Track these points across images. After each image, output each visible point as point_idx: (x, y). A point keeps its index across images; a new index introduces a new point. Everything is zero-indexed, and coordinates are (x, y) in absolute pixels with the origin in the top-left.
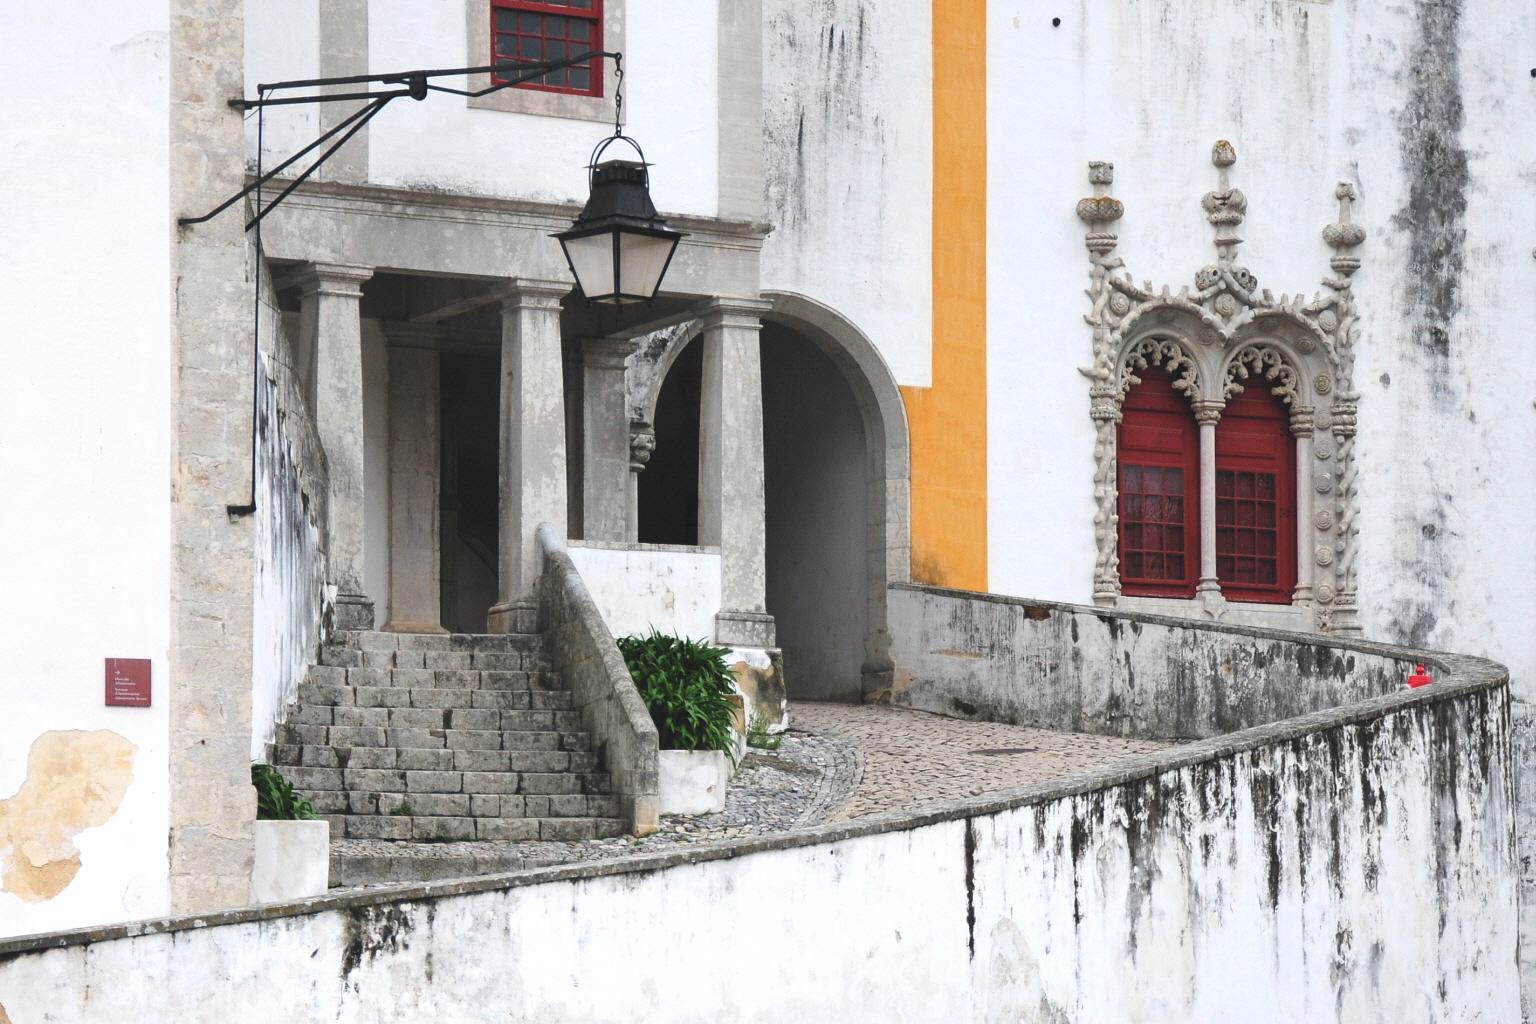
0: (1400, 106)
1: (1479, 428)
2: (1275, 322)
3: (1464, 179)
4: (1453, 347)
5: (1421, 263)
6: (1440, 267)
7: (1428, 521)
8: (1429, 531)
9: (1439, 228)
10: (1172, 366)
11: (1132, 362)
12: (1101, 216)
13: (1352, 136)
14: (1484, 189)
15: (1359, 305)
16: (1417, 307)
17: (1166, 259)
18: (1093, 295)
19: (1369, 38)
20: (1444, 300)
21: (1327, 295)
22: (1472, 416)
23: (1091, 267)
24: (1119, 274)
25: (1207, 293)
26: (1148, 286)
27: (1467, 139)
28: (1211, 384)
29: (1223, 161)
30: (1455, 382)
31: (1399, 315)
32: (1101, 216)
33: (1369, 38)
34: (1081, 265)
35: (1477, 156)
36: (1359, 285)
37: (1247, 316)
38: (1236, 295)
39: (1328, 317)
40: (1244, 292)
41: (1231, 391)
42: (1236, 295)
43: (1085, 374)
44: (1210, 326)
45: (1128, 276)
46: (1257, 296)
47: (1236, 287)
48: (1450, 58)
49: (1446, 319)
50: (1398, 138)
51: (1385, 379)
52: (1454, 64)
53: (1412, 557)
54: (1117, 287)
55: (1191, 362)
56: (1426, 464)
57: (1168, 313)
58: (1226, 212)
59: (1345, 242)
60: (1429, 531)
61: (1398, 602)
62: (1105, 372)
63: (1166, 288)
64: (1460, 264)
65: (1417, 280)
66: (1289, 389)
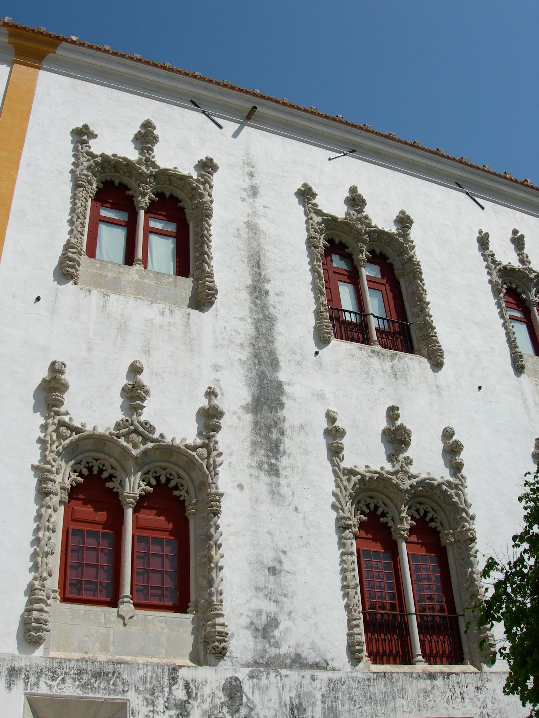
0: (244, 358)
1: (301, 516)
2: (169, 451)
3: (282, 393)
4: (282, 473)
5: (260, 430)
6: (272, 433)
7: (272, 564)
8: (273, 571)
9: (269, 415)
10: (105, 475)
13: (216, 368)
14: (293, 399)
15: (221, 447)
16: (259, 451)
19: (225, 328)
20: (275, 449)
22: (296, 509)
26: (83, 425)
27: (282, 376)
30: (285, 490)
31: (248, 455)
33: (225, 328)
35: (289, 384)
36: (219, 437)
37: (150, 445)
39: (204, 451)
41: (144, 490)
43: (34, 468)
45: (71, 419)
46: (156, 436)
47: (141, 429)
48: (272, 342)
49: (277, 459)
50: (243, 372)
51: (241, 487)
52: (273, 345)
53: (261, 585)
54: (61, 424)
55: (116, 473)
56: (269, 533)
57: (98, 441)
60: (273, 571)
61: (254, 611)
63: (94, 429)
64: (283, 433)
65: (258, 438)
66: (183, 493)
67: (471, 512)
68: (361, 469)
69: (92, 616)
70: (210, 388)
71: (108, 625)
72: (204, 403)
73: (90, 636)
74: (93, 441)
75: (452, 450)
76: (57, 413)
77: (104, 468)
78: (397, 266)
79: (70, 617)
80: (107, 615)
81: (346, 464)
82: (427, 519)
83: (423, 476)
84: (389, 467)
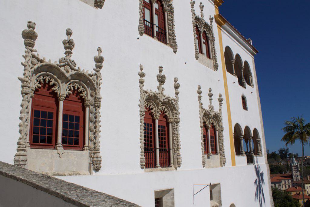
10: (52, 83)
11: (39, 80)
12: (30, 37)
17: (50, 51)
18: (25, 57)
21: (94, 72)
23: (26, 50)
24: (35, 53)
25: (63, 64)
28: (63, 90)
29: (69, 33)
32: (30, 37)
34: (24, 48)
36: (102, 71)
37: (73, 72)
38: (70, 66)
39: (95, 77)
40: (73, 66)
42: (70, 66)
44: (62, 74)
45: (38, 54)
46: (76, 68)
47: (71, 64)
54: (33, 56)
57: (50, 68)
58: (69, 45)
59: (99, 61)
62: (27, 79)
63: (50, 61)
67: (179, 111)
68: (149, 91)
69: (45, 154)
70: (99, 47)
71: (52, 158)
72: (96, 54)
73: (44, 164)
74: (48, 67)
75: (177, 87)
76: (32, 51)
77: (51, 80)
78: (165, 6)
79: (36, 155)
80: (52, 153)
81: (144, 88)
82: (165, 111)
83: (167, 96)
84: (158, 91)
